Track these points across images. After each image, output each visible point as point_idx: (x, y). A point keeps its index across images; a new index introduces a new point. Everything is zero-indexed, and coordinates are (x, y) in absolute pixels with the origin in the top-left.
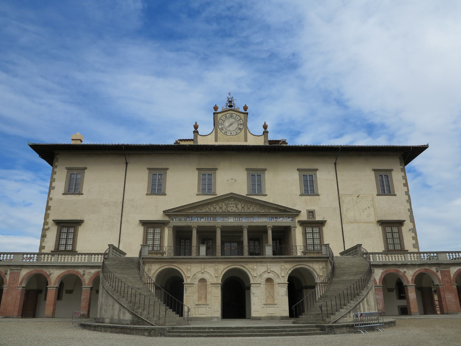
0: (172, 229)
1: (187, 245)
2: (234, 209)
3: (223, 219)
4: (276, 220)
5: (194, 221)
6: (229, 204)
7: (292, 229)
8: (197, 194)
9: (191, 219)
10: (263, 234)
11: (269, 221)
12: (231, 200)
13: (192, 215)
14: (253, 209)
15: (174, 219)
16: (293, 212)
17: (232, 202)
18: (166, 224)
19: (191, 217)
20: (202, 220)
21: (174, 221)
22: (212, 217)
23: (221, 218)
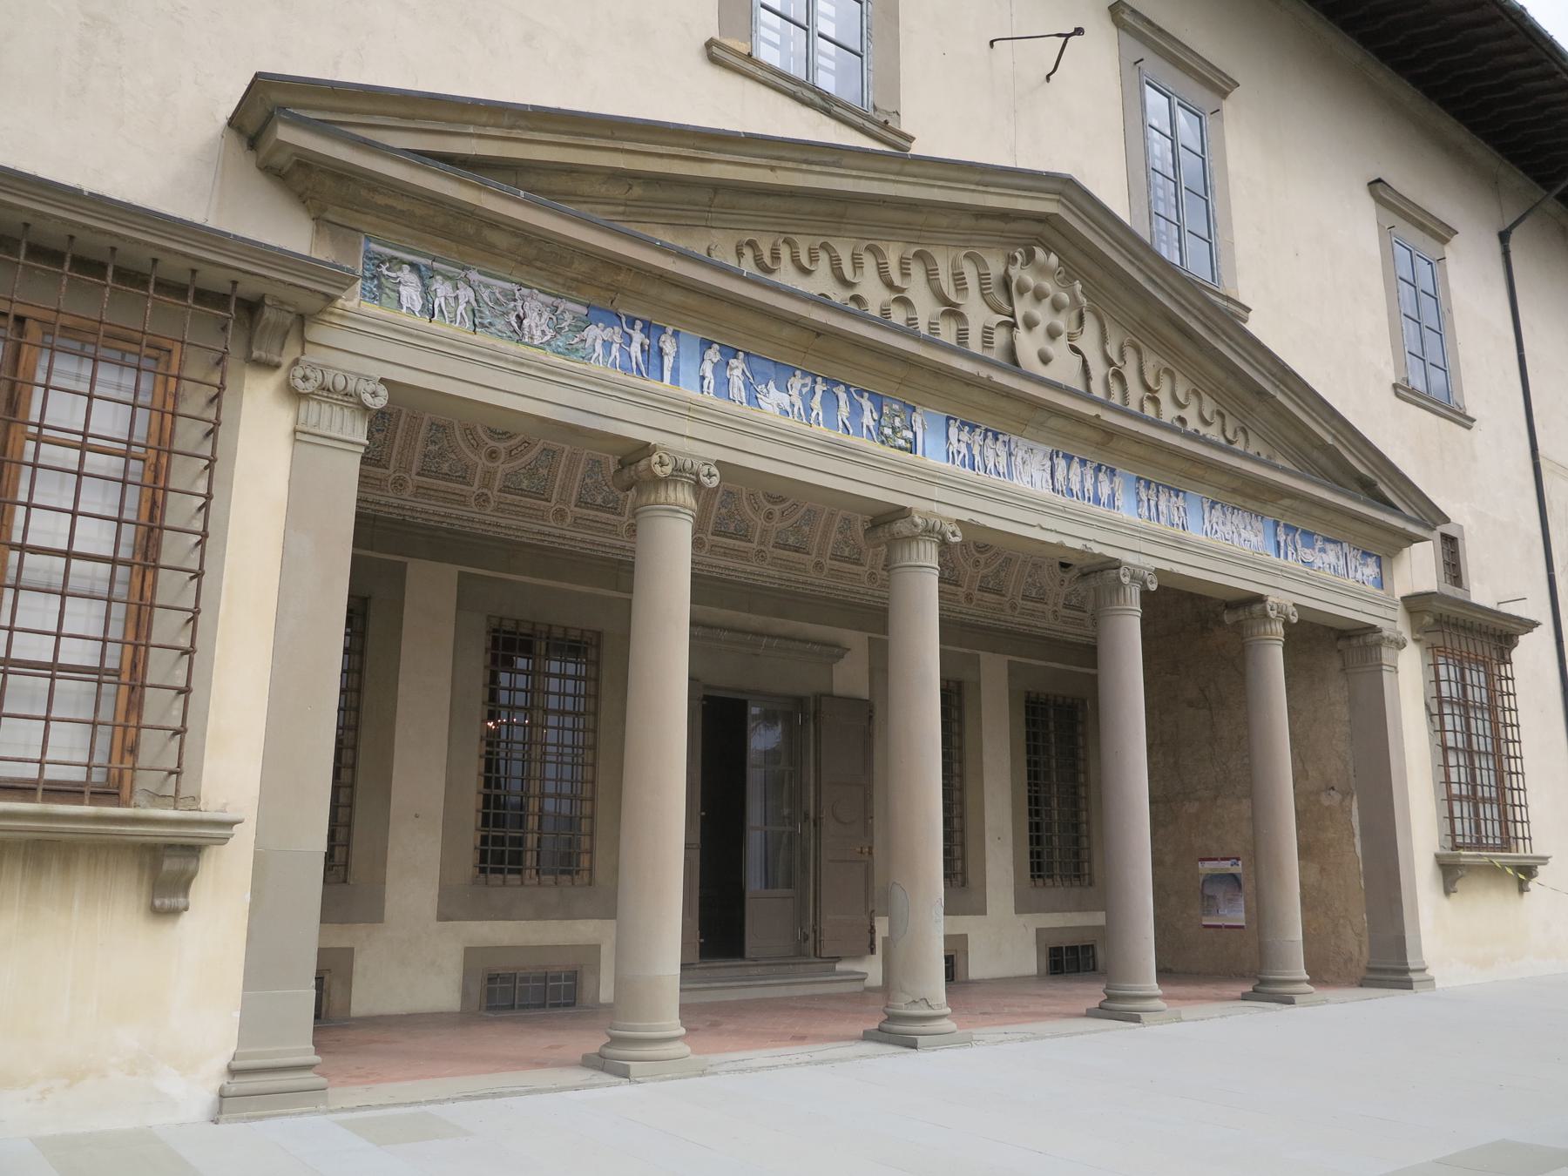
0: (358, 432)
1: (553, 702)
2: (1064, 369)
3: (968, 445)
4: (1308, 555)
5: (675, 380)
6: (1022, 290)
7: (1386, 654)
8: (710, 44)
9: (635, 350)
10: (984, 656)
11: (1273, 557)
12: (1040, 253)
13: (674, 296)
14: (1183, 414)
15: (406, 274)
16: (1407, 512)
17: (1048, 285)
18: (269, 314)
19: (647, 328)
20: (773, 399)
21: (403, 317)
22: (878, 401)
23: (953, 431)
